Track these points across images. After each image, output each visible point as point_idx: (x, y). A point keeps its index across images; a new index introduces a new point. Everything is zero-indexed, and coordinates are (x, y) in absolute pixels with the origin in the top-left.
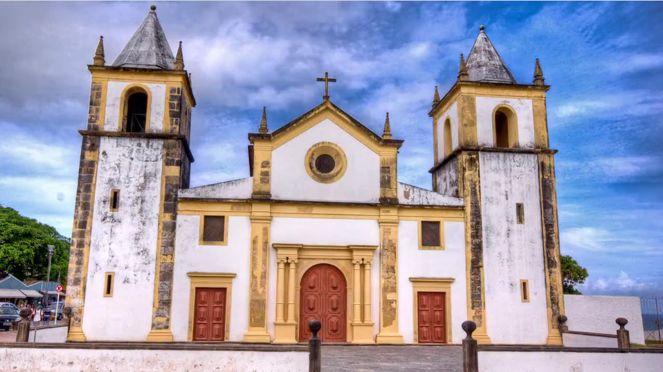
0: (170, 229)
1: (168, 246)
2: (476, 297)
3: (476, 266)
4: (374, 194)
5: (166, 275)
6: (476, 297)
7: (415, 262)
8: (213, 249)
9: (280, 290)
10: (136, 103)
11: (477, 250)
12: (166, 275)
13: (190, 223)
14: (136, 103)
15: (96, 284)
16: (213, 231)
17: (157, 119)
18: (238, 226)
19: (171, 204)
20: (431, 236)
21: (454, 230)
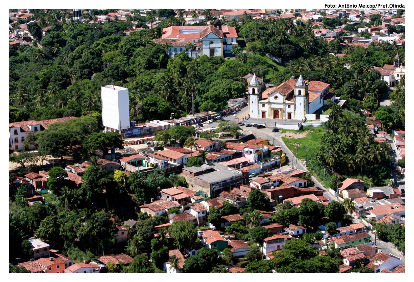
0: (259, 105)
1: (259, 107)
2: (295, 114)
3: (295, 110)
4: (282, 102)
5: (259, 111)
6: (295, 114)
7: (288, 110)
8: (263, 108)
9: (272, 112)
10: (254, 90)
11: (295, 108)
12: (259, 111)
13: (261, 105)
14: (254, 90)
15: (251, 112)
16: (263, 105)
17: (256, 92)
18: (266, 105)
19: (258, 103)
20: (289, 106)
21: (292, 106)
